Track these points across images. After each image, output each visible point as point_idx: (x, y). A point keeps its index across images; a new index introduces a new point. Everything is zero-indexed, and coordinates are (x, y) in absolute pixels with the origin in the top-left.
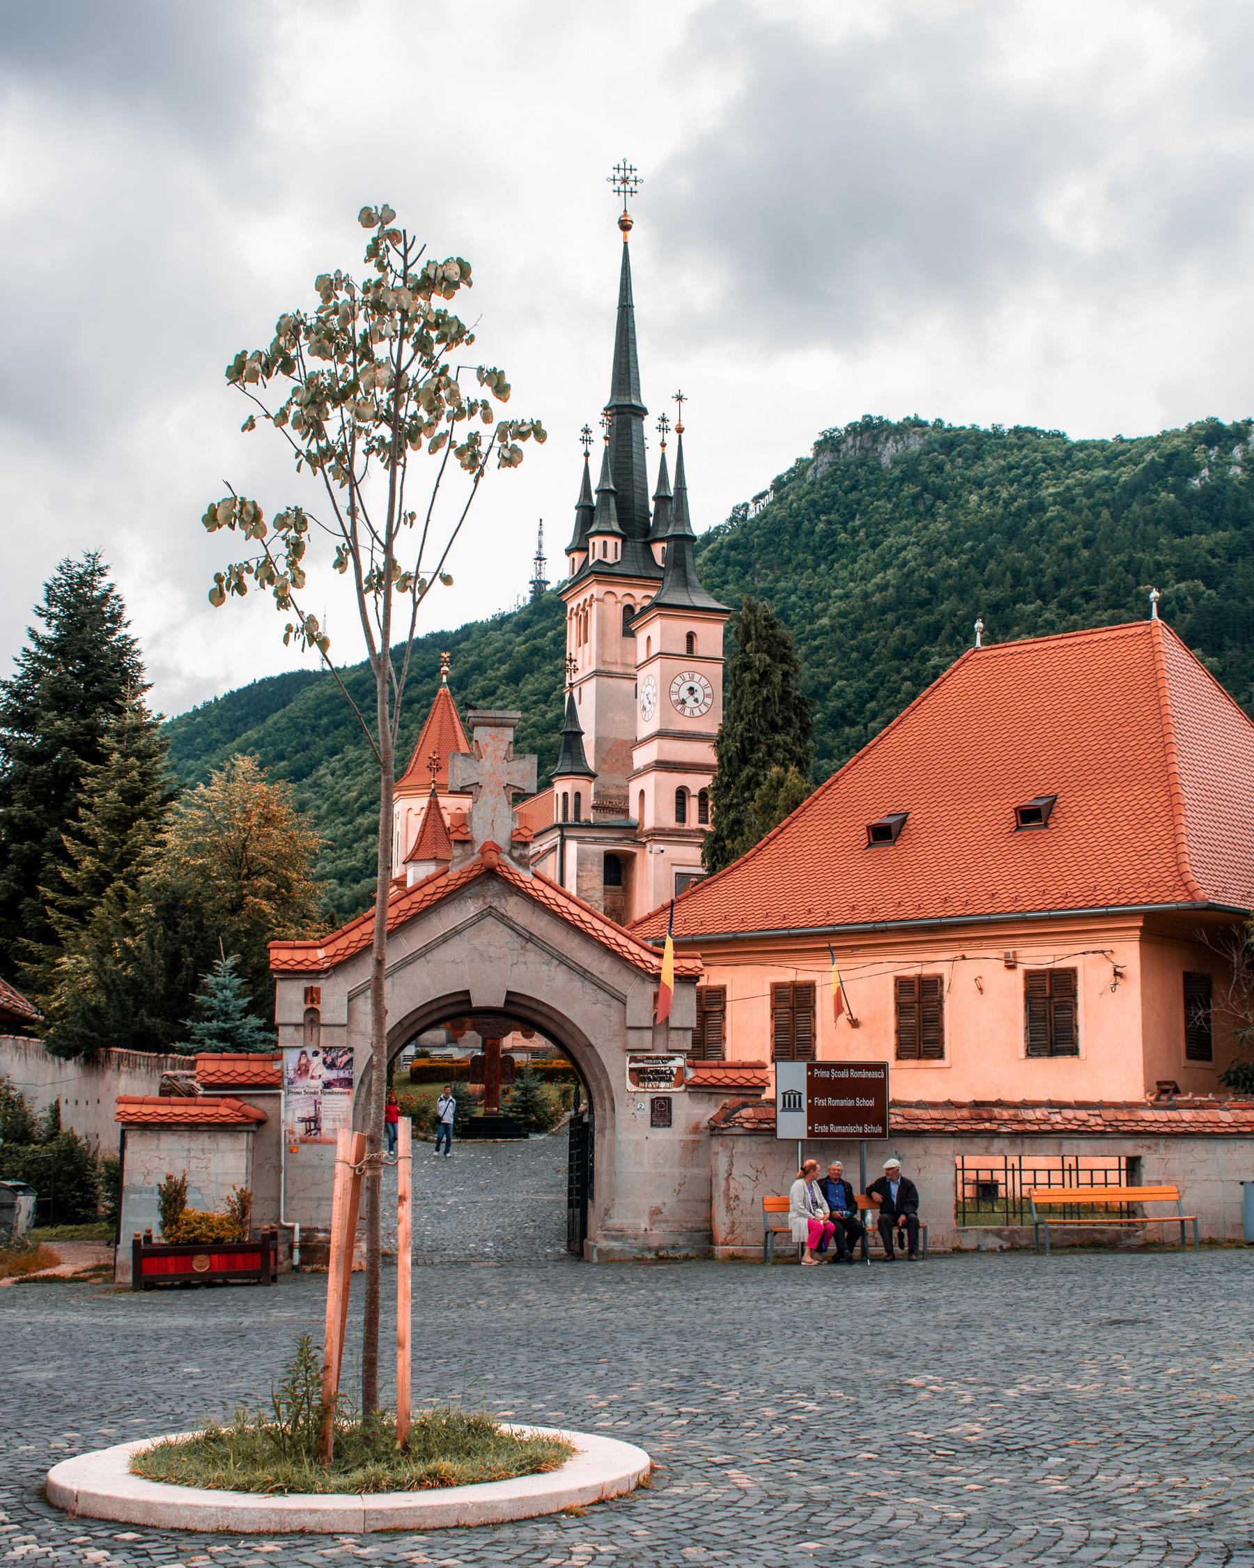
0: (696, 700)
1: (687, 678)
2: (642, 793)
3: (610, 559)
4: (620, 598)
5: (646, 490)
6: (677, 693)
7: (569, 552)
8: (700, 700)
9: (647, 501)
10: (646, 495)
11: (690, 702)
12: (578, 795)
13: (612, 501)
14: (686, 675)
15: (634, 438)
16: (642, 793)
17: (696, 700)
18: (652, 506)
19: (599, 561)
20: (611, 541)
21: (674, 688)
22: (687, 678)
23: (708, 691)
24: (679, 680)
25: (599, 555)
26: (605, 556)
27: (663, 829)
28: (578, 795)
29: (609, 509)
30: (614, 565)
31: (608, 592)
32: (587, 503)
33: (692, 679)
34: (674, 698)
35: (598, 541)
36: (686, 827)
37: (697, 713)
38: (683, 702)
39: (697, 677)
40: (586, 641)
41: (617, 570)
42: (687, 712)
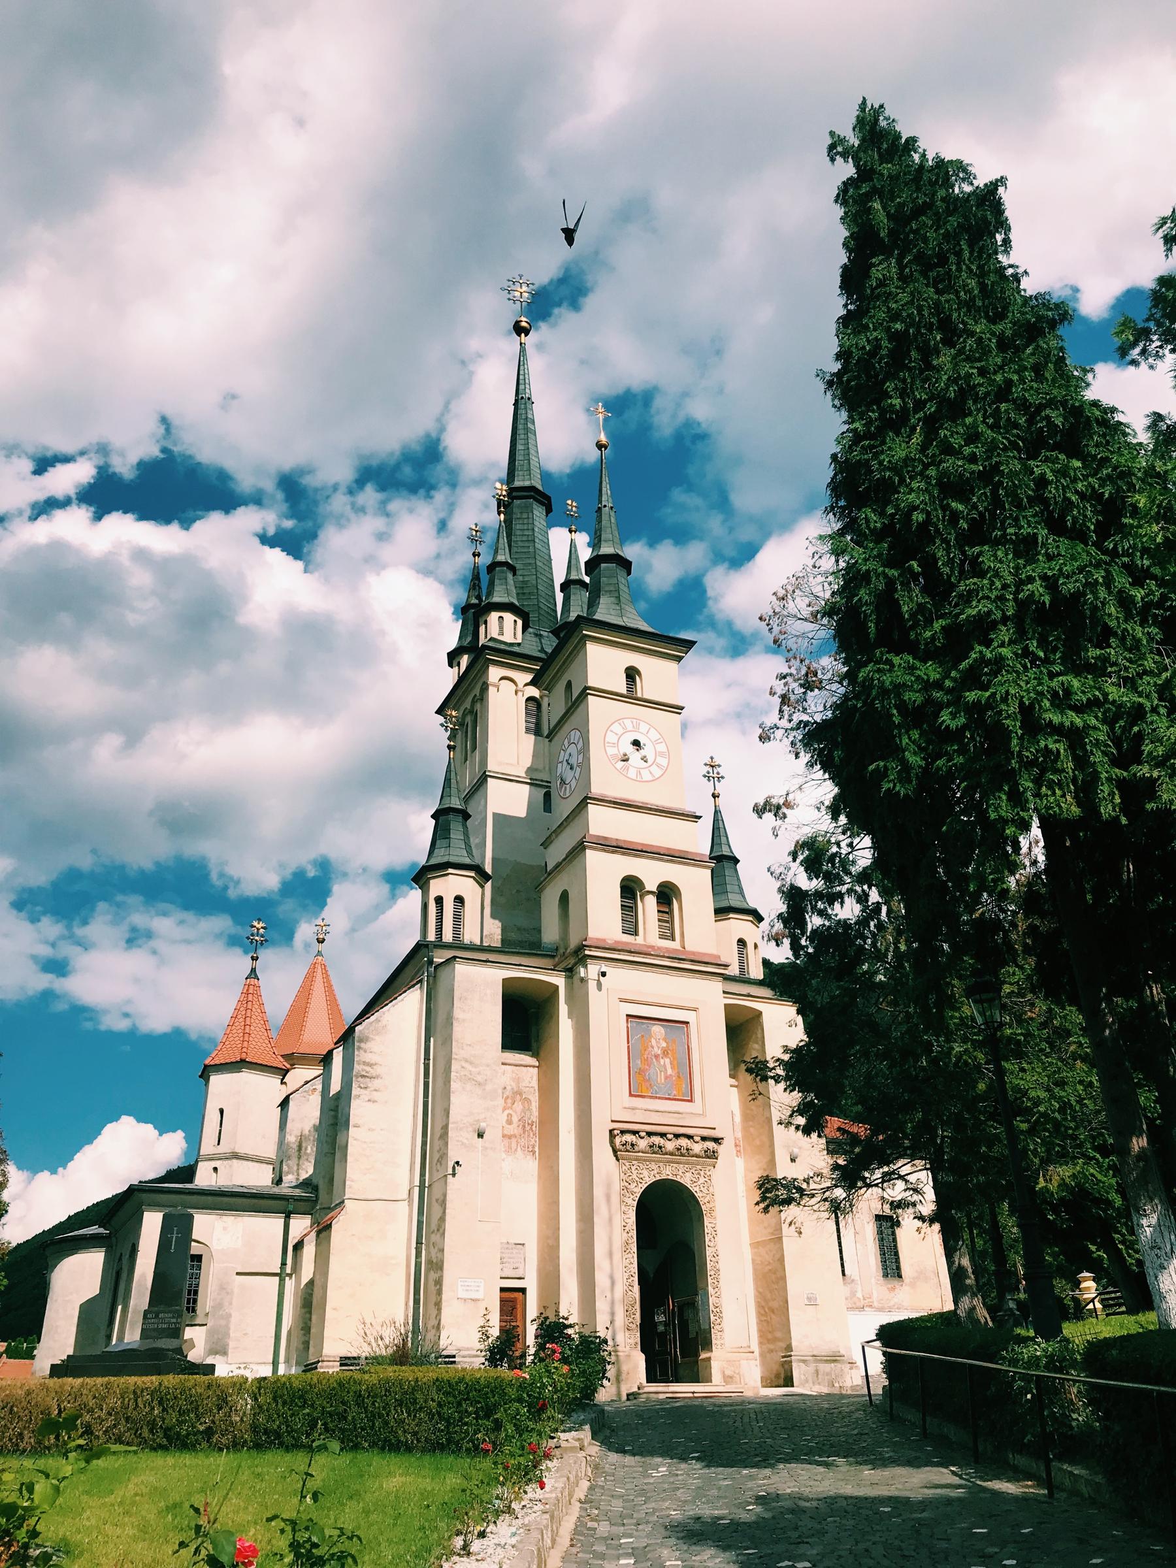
0: (644, 759)
1: (630, 727)
2: (564, 898)
3: (508, 638)
4: (521, 685)
5: (552, 580)
6: (616, 745)
7: (453, 657)
8: (650, 759)
9: (554, 592)
10: (553, 587)
11: (635, 756)
12: (459, 900)
13: (510, 576)
14: (628, 722)
15: (536, 523)
16: (564, 898)
17: (644, 759)
18: (559, 597)
19: (492, 639)
20: (509, 617)
21: (611, 738)
22: (630, 727)
23: (661, 748)
24: (616, 728)
25: (494, 632)
26: (501, 633)
27: (604, 940)
28: (459, 900)
29: (506, 584)
30: (512, 645)
31: (502, 678)
32: (474, 601)
33: (636, 729)
34: (611, 751)
35: (494, 616)
36: (639, 940)
37: (646, 776)
38: (625, 760)
39: (644, 727)
40: (474, 748)
41: (516, 649)
42: (632, 773)
